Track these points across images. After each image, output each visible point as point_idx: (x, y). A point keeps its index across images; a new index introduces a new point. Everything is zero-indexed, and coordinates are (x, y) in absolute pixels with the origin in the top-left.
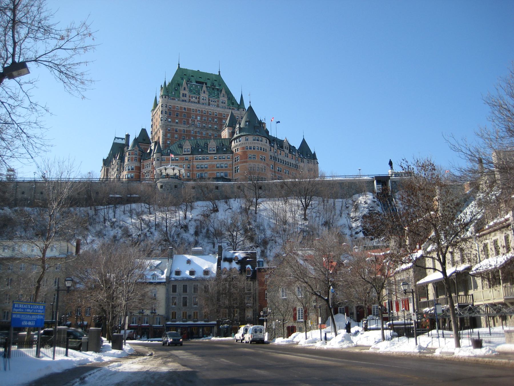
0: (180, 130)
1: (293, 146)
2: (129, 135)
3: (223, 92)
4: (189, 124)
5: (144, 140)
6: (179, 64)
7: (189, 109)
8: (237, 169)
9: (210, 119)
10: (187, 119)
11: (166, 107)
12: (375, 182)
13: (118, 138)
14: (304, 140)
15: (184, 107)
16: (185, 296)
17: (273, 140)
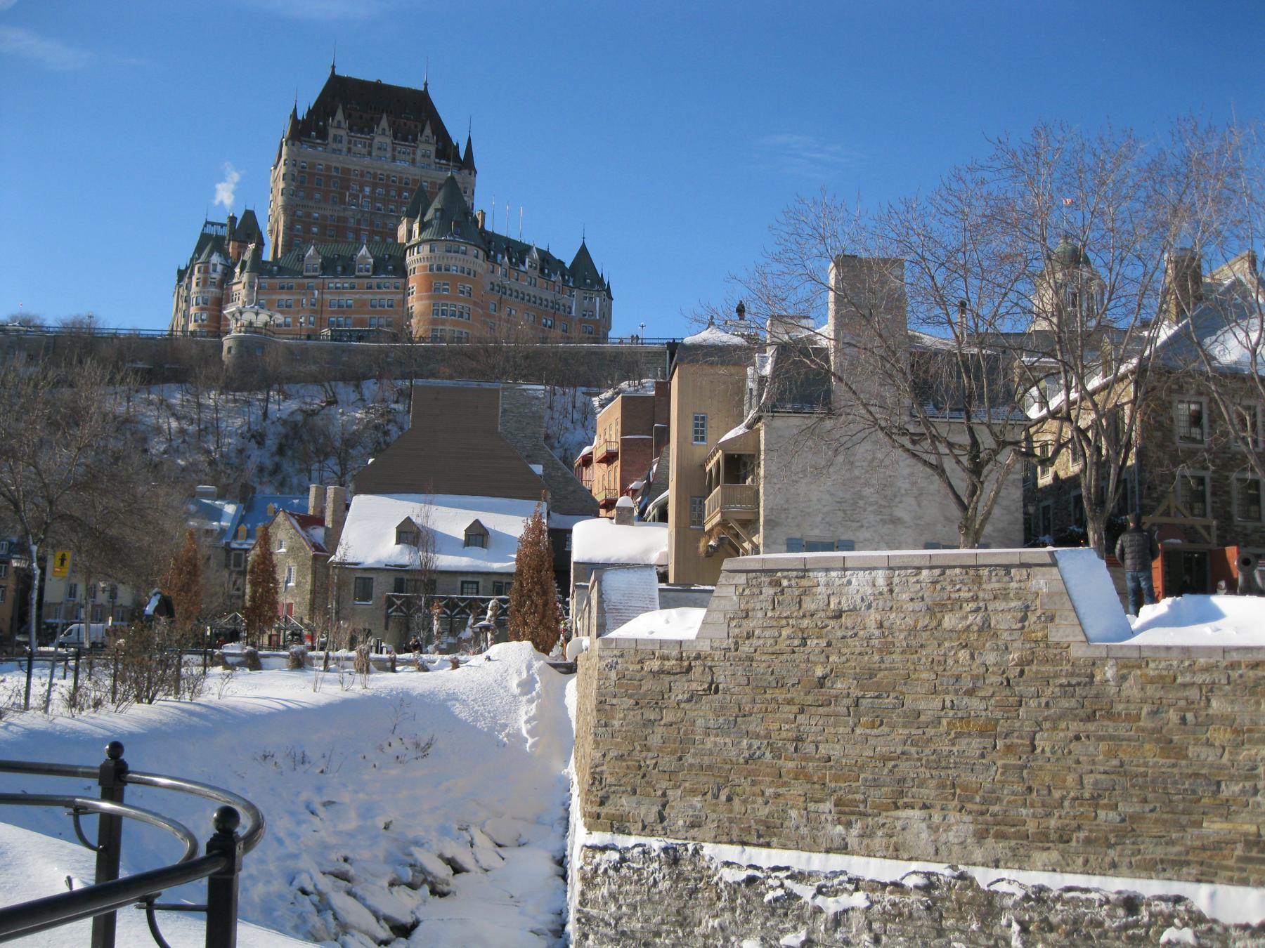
0: (324, 217)
1: (559, 261)
3: (428, 131)
6: (333, 67)
7: (347, 171)
9: (393, 193)
11: (295, 165)
13: (213, 224)
15: (333, 164)
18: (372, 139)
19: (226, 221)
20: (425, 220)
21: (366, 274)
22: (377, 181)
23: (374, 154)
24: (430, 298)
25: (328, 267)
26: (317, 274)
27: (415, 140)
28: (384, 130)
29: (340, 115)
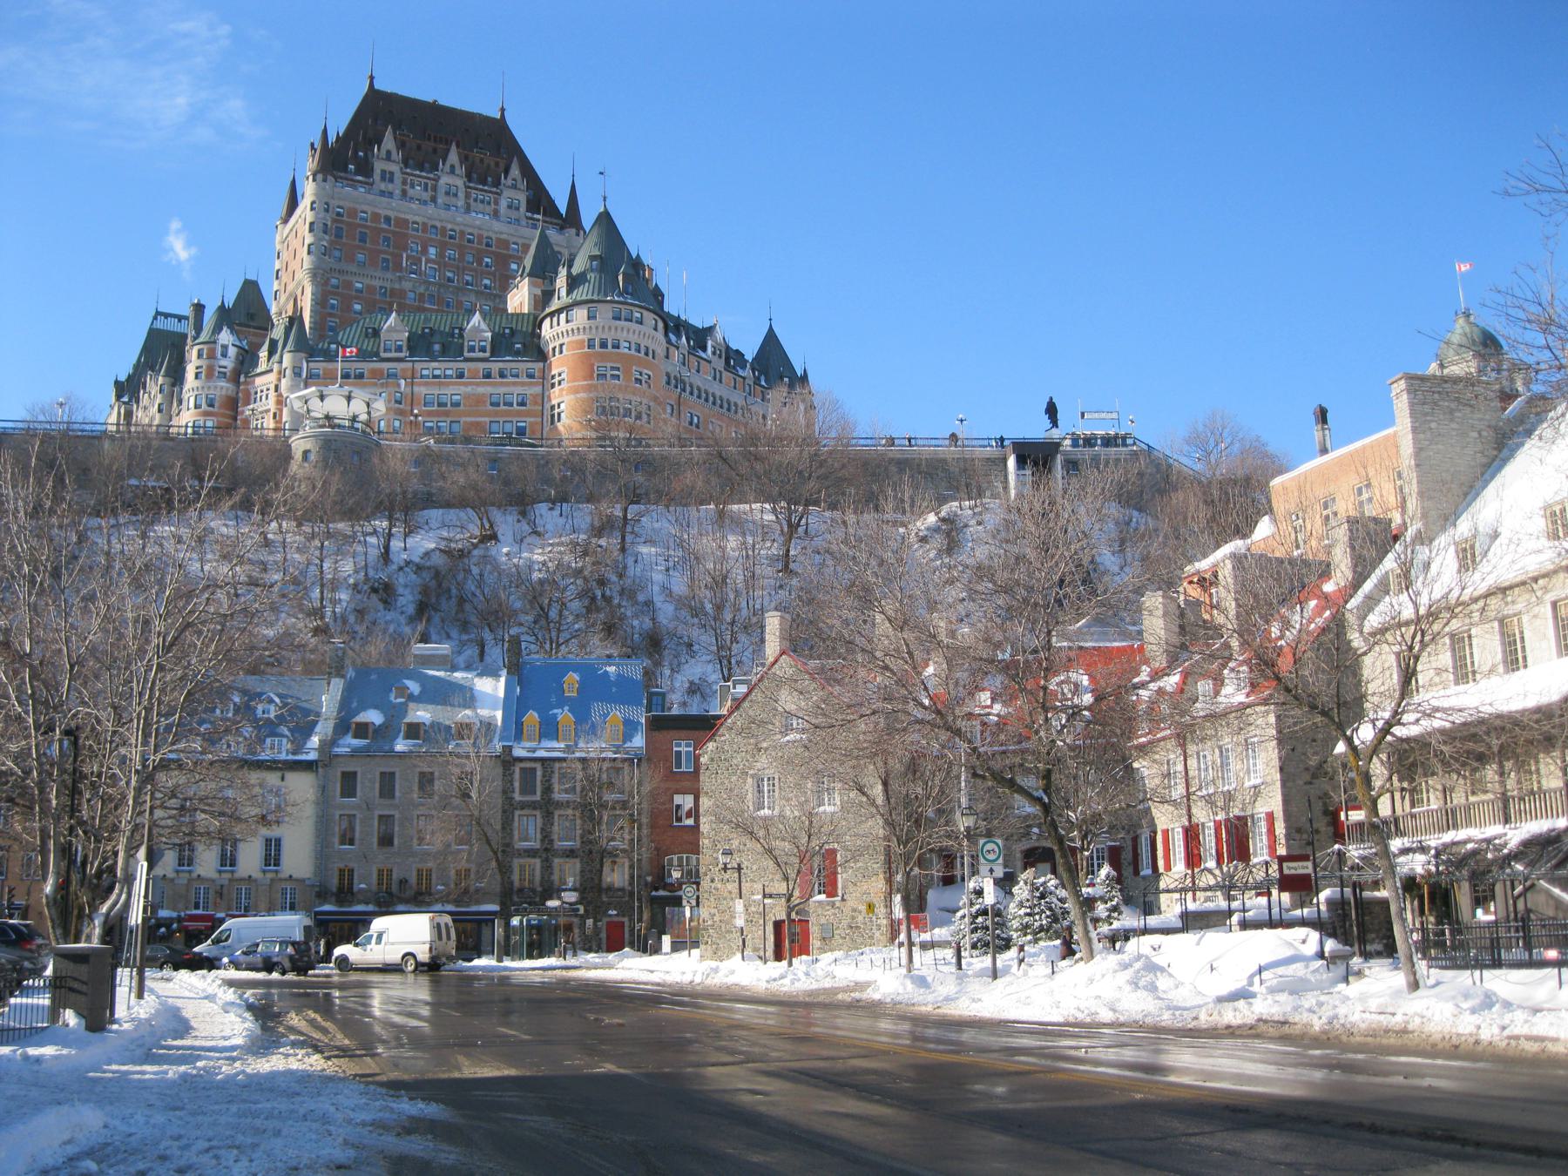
0: (371, 289)
1: (737, 352)
2: (204, 307)
3: (515, 171)
4: (401, 271)
5: (251, 316)
6: (372, 78)
7: (403, 223)
8: (556, 411)
9: (469, 258)
10: (392, 254)
11: (327, 210)
12: (1011, 462)
13: (167, 316)
14: (771, 332)
15: (383, 212)
16: (386, 812)
17: (675, 326)
18: (437, 180)
19: (187, 311)
20: (575, 271)
21: (481, 355)
22: (446, 239)
23: (440, 201)
24: (589, 389)
25: (420, 345)
26: (402, 355)
27: (497, 183)
28: (452, 167)
29: (389, 142)
